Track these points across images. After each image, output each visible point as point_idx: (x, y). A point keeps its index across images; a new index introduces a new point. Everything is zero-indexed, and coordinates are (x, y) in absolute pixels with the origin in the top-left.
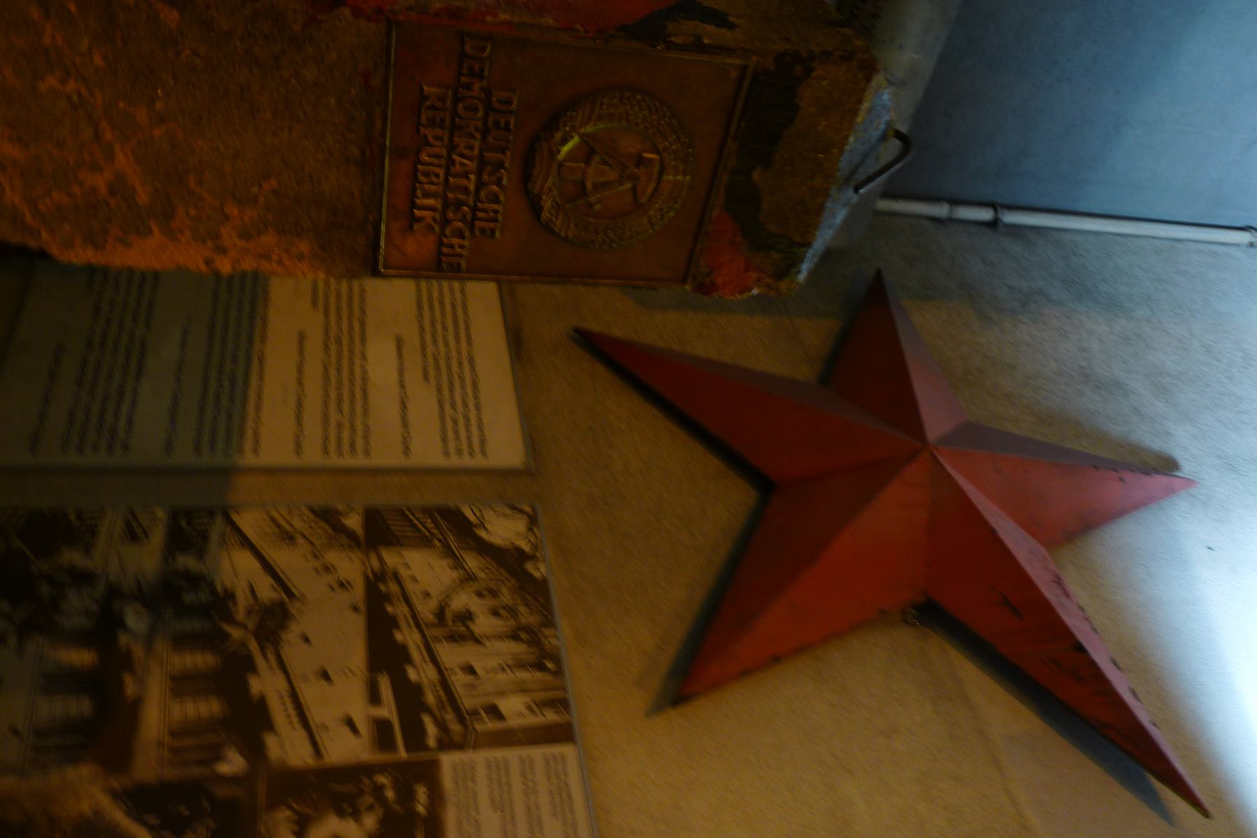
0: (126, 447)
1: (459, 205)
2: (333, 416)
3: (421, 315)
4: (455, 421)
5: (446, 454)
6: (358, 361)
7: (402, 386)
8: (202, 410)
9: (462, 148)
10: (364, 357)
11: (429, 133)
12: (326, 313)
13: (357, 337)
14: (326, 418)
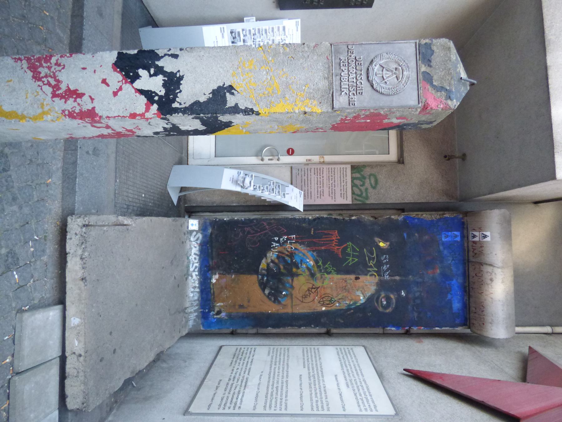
0: (240, 407)
1: (353, 86)
2: (314, 399)
3: (343, 369)
4: (362, 400)
5: (361, 410)
6: (321, 382)
7: (339, 389)
8: (266, 397)
9: (351, 71)
10: (323, 381)
11: (343, 68)
12: (309, 369)
13: (320, 375)
14: (311, 400)
